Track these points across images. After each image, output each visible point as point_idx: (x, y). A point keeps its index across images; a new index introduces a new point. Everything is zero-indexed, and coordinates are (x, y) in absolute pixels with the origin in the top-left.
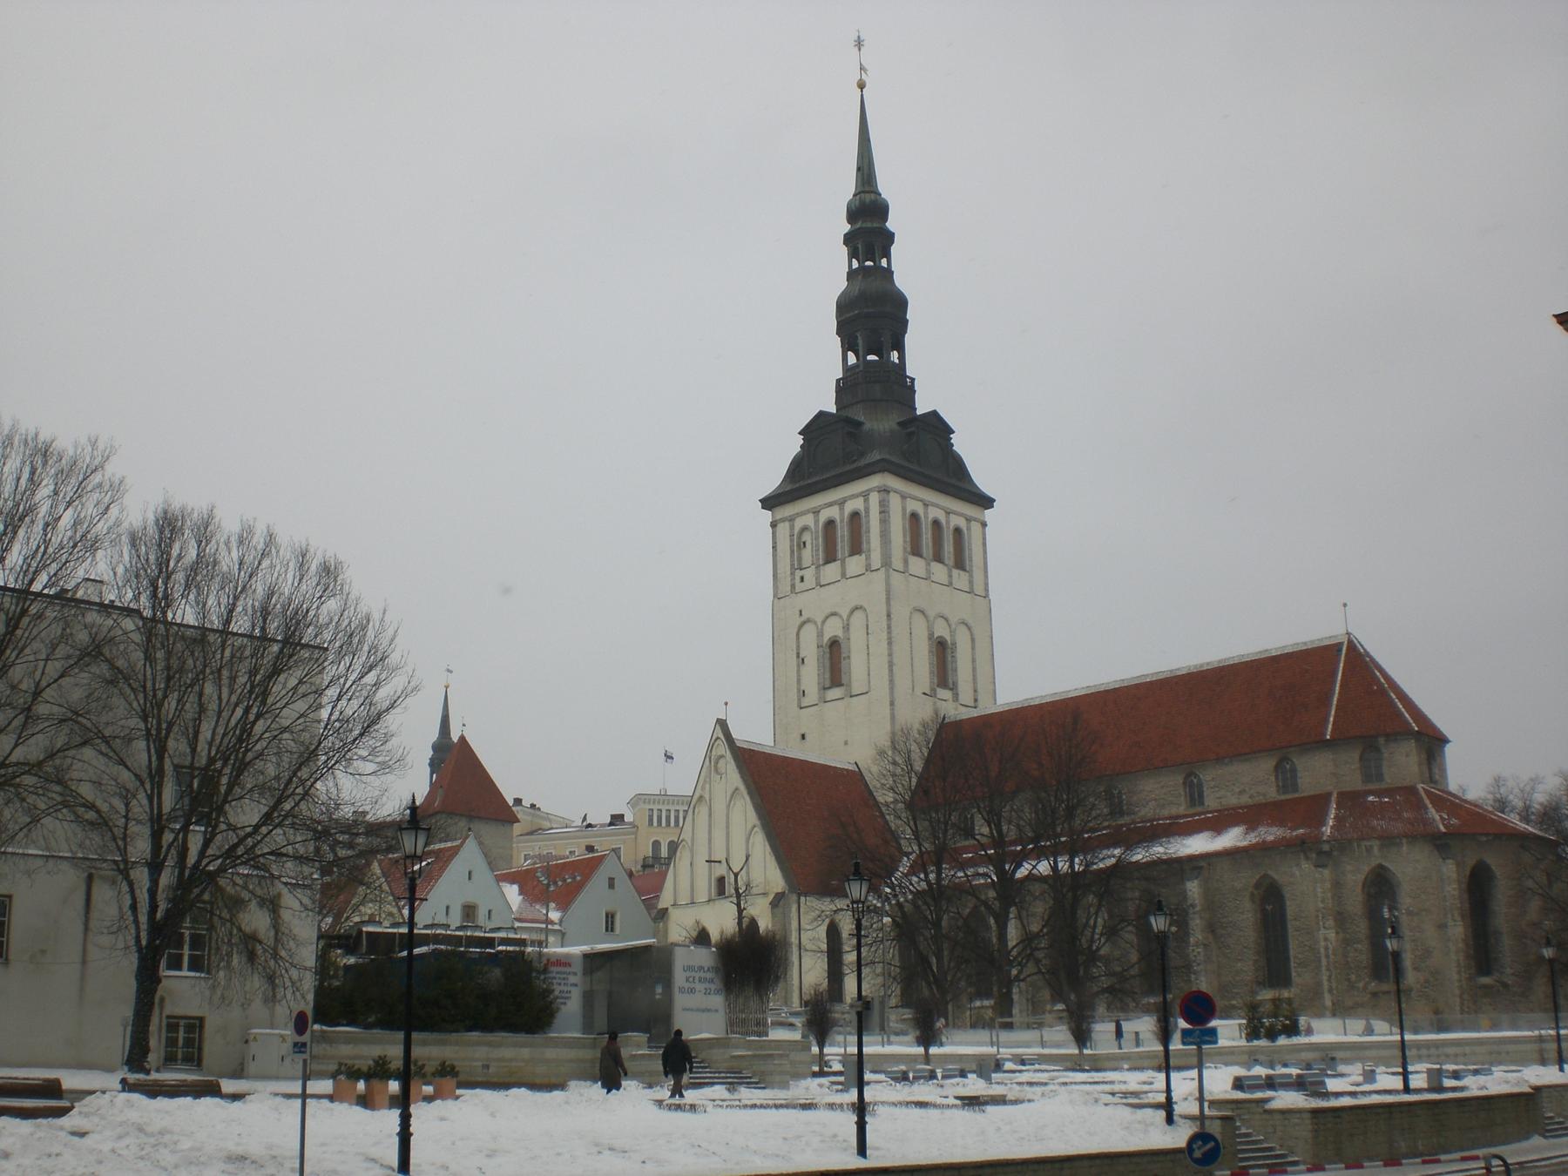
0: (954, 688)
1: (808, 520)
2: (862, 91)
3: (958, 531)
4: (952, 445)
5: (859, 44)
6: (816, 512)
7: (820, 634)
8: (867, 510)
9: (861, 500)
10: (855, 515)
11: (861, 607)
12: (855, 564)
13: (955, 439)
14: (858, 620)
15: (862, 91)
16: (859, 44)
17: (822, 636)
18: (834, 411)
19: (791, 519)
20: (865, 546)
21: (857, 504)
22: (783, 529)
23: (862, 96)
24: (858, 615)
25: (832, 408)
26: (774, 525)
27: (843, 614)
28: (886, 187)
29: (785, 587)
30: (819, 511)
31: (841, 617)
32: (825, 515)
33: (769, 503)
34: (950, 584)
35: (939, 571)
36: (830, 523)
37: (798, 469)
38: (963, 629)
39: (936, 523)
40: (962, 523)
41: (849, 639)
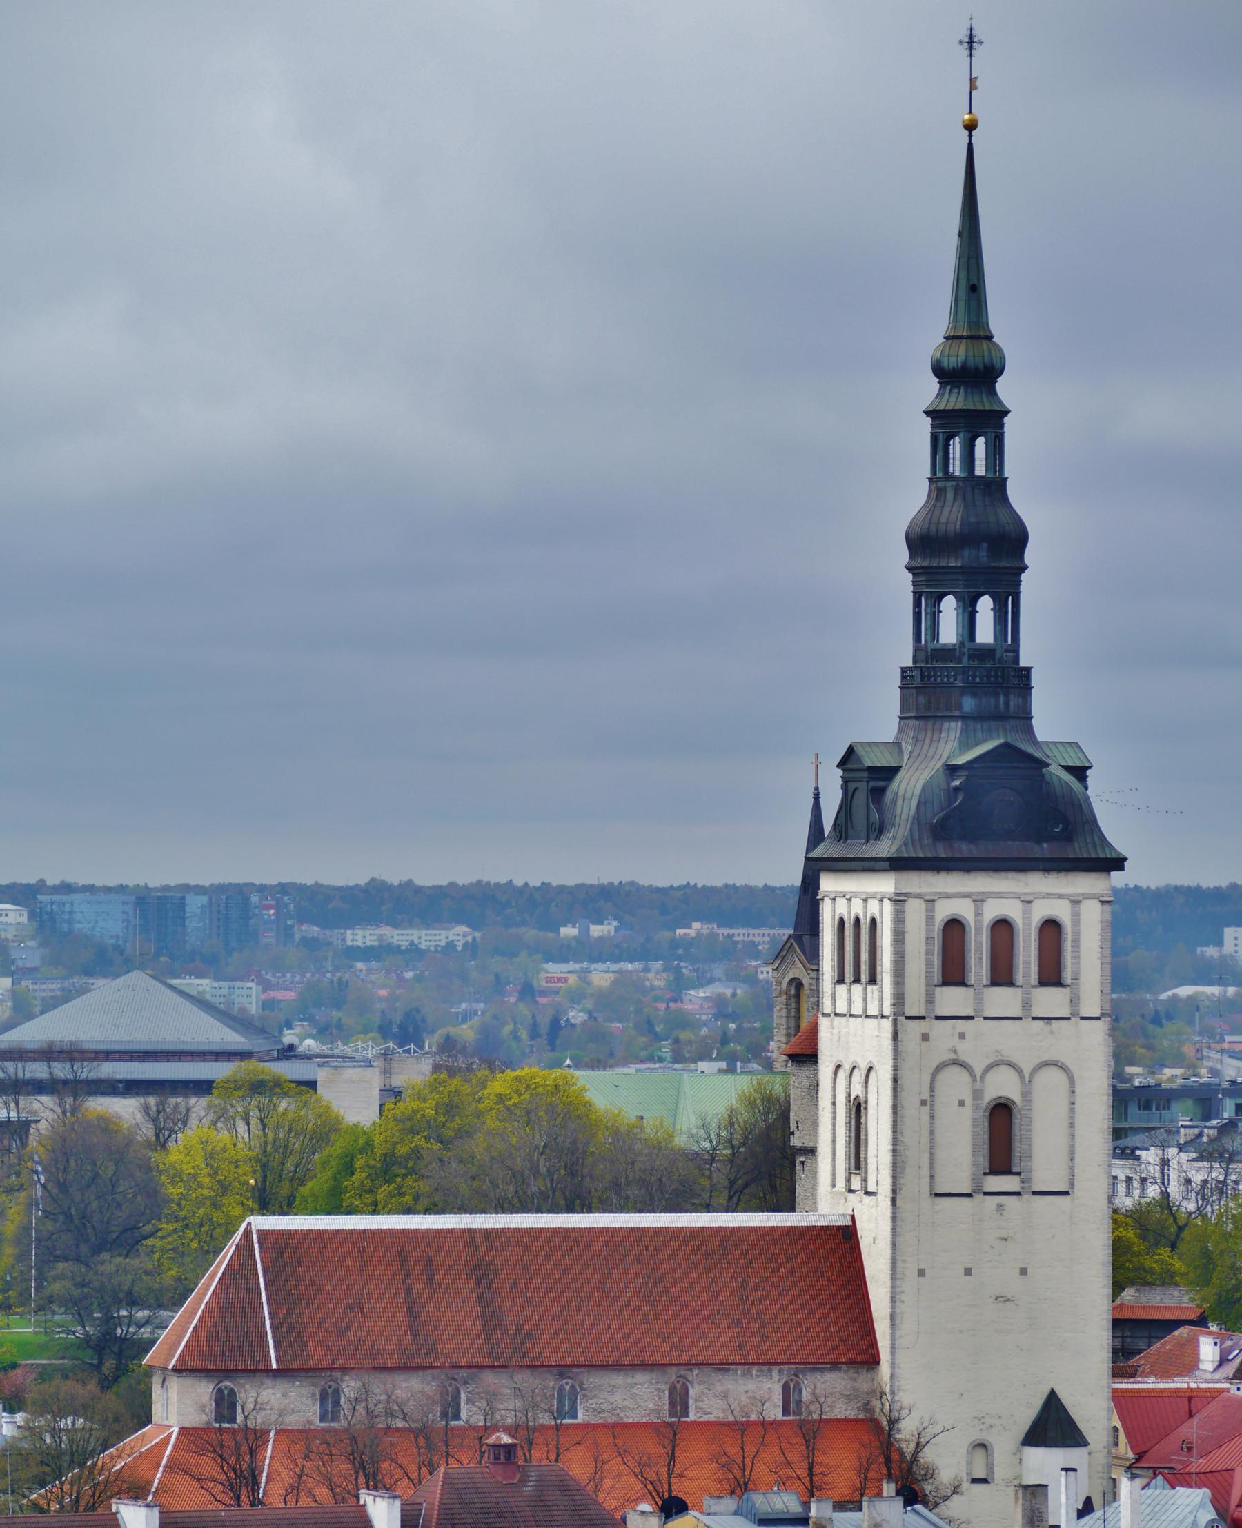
1: (964, 910)
2: (970, 136)
6: (979, 900)
7: (977, 1094)
8: (1076, 921)
11: (1063, 1068)
12: (1050, 1000)
14: (1050, 1083)
15: (970, 136)
17: (982, 1099)
20: (1067, 976)
21: (1062, 912)
22: (915, 909)
23: (970, 145)
27: (1025, 1071)
29: (914, 1006)
30: (983, 901)
31: (1019, 1071)
32: (992, 911)
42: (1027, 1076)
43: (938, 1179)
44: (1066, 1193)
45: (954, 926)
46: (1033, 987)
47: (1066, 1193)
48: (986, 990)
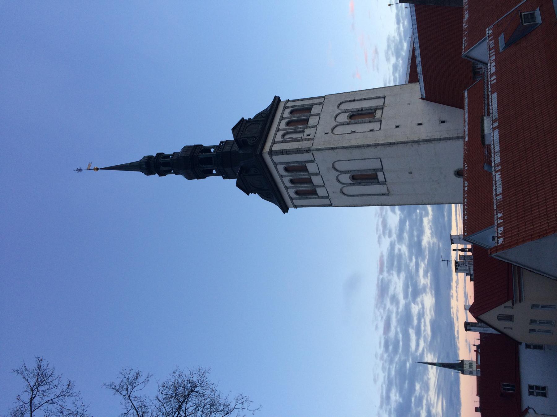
0: (376, 109)
1: (292, 192)
2: (99, 169)
3: (291, 112)
4: (250, 119)
5: (79, 170)
6: (287, 188)
8: (281, 164)
9: (278, 167)
10: (286, 169)
12: (311, 168)
13: (246, 118)
14: (341, 166)
15: (99, 169)
16: (79, 170)
18: (236, 179)
19: (292, 199)
21: (281, 168)
23: (101, 169)
24: (336, 165)
25: (234, 181)
26: (296, 207)
28: (137, 158)
29: (326, 201)
30: (287, 187)
32: (289, 184)
33: (285, 209)
34: (319, 115)
35: (312, 121)
36: (292, 181)
37: (266, 196)
38: (343, 107)
39: (288, 124)
40: (287, 111)
41: (351, 171)
42: (340, 173)
43: (383, 192)
44: (381, 160)
45: (297, 193)
46: (309, 173)
47: (381, 160)
48: (314, 184)
